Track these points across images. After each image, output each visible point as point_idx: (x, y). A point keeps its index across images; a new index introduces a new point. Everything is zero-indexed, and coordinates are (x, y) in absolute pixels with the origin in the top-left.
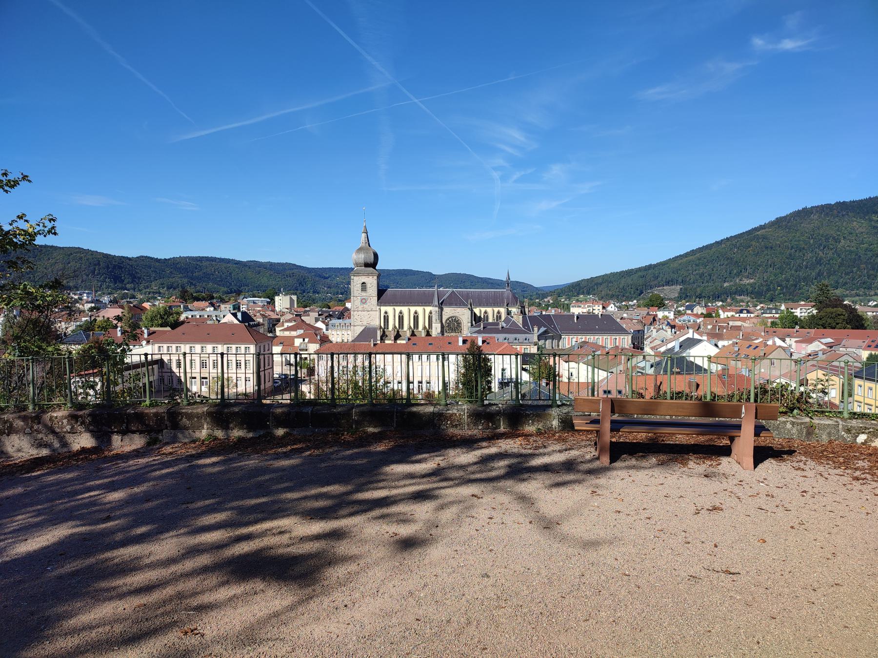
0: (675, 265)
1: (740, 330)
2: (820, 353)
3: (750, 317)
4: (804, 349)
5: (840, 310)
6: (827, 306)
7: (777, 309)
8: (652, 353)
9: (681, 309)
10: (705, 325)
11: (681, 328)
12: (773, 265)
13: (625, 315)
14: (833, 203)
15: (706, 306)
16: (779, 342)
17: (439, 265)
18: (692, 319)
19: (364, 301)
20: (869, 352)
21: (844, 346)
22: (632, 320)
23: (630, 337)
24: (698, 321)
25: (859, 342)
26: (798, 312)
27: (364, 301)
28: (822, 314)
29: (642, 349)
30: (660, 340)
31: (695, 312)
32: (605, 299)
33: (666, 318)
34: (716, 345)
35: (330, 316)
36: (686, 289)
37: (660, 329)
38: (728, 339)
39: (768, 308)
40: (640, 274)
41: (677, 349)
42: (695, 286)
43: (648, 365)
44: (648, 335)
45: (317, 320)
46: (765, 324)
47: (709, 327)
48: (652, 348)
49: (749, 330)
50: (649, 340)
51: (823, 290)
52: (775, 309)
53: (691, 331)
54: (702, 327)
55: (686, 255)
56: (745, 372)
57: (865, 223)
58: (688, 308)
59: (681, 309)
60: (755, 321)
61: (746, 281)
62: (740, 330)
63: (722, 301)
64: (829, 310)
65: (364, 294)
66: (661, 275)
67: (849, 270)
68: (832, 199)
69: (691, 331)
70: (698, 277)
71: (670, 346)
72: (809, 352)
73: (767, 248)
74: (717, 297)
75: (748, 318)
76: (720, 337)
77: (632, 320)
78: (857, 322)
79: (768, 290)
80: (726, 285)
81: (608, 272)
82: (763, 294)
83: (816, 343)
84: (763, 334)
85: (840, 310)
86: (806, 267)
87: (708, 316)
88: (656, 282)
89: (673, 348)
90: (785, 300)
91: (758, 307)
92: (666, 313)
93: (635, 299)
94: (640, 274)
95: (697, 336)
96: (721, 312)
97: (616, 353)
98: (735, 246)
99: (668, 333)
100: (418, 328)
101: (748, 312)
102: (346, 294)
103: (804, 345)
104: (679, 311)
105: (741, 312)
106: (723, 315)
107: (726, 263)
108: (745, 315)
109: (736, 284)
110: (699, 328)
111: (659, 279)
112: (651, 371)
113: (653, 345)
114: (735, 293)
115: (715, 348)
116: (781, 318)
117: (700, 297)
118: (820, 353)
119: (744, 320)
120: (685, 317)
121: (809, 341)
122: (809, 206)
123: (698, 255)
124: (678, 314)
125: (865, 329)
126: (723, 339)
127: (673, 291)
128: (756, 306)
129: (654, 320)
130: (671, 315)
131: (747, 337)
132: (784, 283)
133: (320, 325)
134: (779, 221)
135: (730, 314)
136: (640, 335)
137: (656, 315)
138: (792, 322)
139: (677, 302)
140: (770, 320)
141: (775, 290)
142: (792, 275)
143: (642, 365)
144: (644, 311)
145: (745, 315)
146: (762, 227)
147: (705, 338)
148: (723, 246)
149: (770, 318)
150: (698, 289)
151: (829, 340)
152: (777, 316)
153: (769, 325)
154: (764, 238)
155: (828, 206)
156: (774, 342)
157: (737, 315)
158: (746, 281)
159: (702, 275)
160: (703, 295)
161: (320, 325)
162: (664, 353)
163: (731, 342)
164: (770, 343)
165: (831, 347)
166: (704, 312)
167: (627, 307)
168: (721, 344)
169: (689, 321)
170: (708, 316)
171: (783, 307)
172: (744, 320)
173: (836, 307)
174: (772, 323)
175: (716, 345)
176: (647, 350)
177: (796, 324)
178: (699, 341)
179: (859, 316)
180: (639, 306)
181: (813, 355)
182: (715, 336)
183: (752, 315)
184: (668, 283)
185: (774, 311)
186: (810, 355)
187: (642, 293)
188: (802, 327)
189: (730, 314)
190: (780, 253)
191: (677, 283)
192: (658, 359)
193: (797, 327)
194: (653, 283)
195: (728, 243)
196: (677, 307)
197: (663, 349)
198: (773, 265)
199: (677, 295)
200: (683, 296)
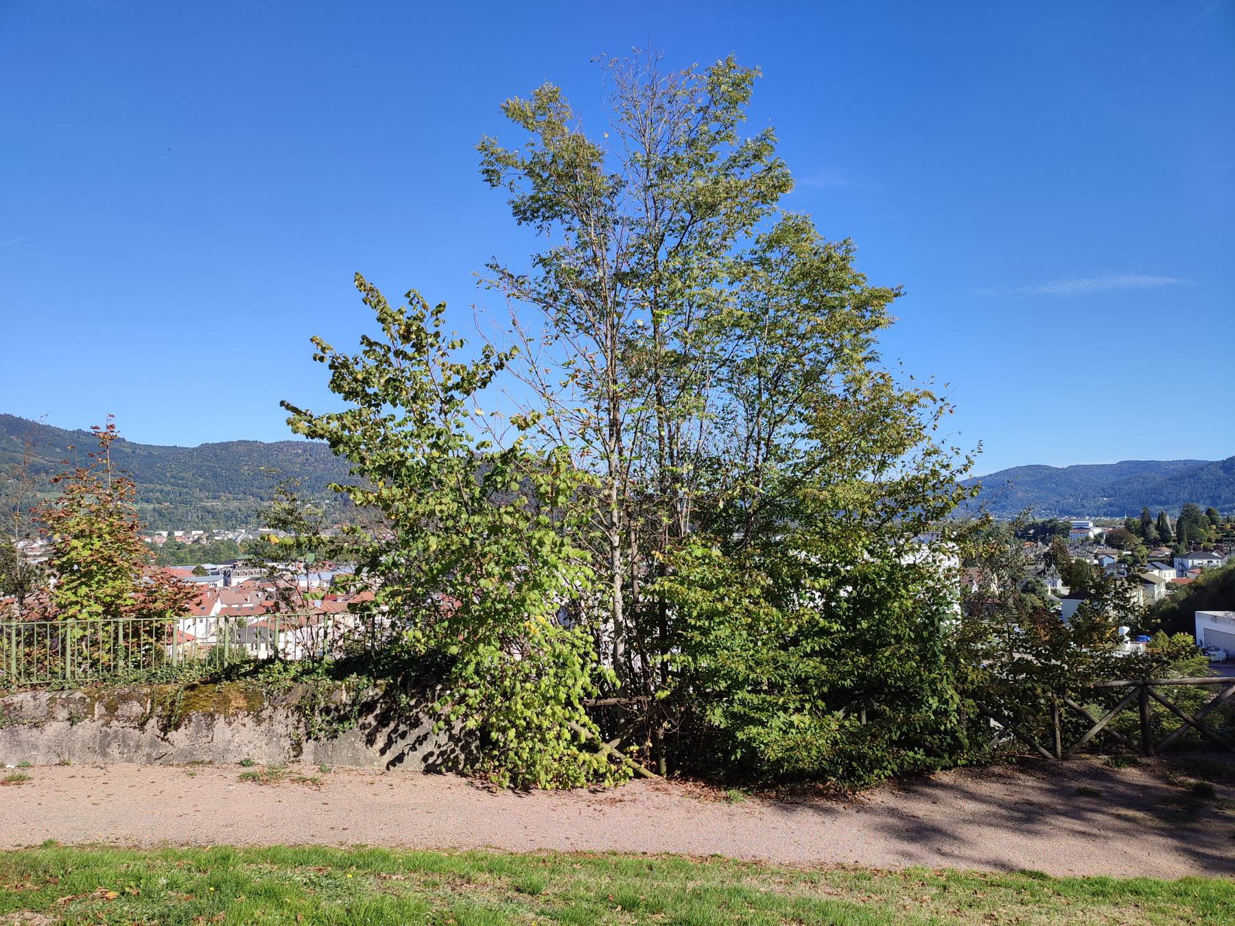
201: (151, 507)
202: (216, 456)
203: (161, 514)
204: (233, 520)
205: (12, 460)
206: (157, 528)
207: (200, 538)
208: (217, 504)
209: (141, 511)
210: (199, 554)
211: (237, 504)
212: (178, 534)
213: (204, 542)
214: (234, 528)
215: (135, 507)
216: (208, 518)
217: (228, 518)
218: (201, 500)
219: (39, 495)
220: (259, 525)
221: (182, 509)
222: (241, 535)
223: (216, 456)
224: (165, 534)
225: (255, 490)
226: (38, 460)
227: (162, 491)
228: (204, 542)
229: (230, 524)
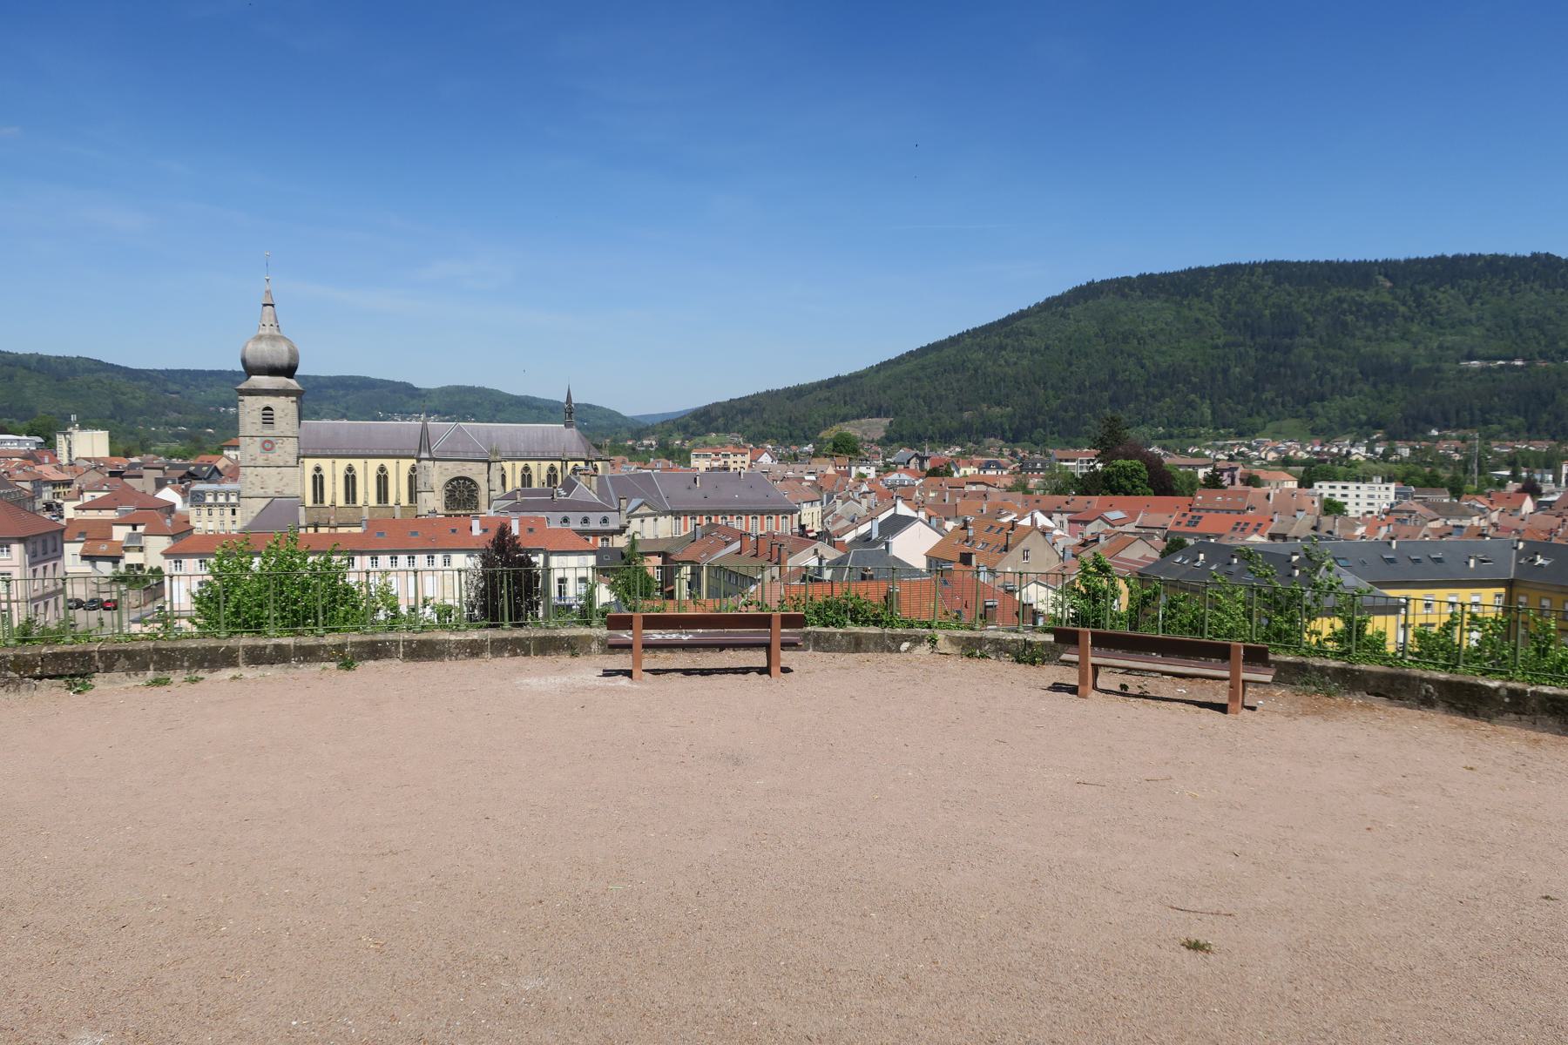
14: (1134, 276)
17: (428, 377)
19: (268, 445)
27: (268, 445)
32: (757, 439)
35: (192, 476)
37: (849, 498)
45: (160, 484)
55: (900, 360)
65: (268, 432)
68: (1132, 270)
74: (947, 439)
81: (762, 390)
92: (863, 470)
100: (386, 501)
102: (229, 432)
105: (987, 466)
122: (1097, 280)
127: (878, 427)
130: (871, 472)
133: (168, 495)
134: (1050, 304)
146: (1022, 315)
155: (1127, 281)
161: (168, 495)
167: (795, 458)
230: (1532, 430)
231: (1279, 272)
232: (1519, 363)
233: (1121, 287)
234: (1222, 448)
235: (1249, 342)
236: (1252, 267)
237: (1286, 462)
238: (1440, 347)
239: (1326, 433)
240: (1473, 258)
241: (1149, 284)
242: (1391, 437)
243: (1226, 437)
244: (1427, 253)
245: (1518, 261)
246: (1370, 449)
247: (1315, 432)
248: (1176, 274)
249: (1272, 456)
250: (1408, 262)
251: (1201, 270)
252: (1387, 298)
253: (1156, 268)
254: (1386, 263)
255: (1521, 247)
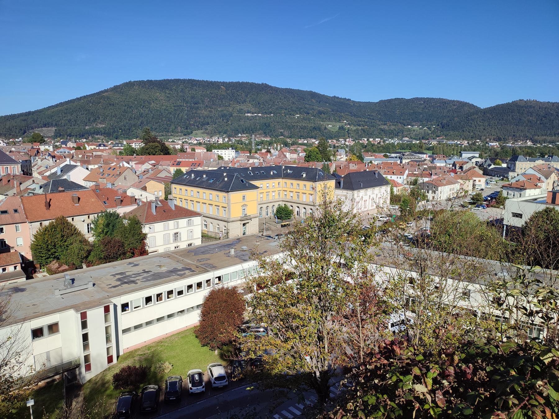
0: (49, 112)
1: (101, 157)
2: (150, 170)
3: (106, 149)
4: (140, 168)
5: (157, 144)
6: (150, 142)
7: (122, 144)
8: (40, 177)
9: (58, 144)
10: (77, 155)
11: (60, 157)
12: (115, 116)
13: (13, 149)
15: (75, 142)
16: (126, 165)
18: (67, 151)
20: (175, 168)
21: (161, 165)
22: (19, 152)
23: (19, 166)
24: (71, 152)
25: (168, 162)
26: (133, 145)
28: (148, 146)
29: (31, 174)
30: (44, 167)
31: (68, 146)
33: (47, 150)
34: (87, 169)
36: (59, 130)
38: (94, 164)
39: (116, 143)
40: (22, 118)
41: (59, 173)
42: (66, 128)
43: (37, 187)
44: (34, 164)
46: (117, 155)
47: (80, 156)
48: (39, 173)
49: (107, 158)
50: (36, 167)
51: (147, 132)
52: (121, 144)
53: (68, 159)
54: (75, 156)
55: (57, 106)
56: (109, 186)
57: (163, 94)
58: (63, 143)
59: (58, 144)
60: (109, 151)
61: (100, 126)
62: (101, 157)
63: (86, 139)
64: (151, 144)
66: (39, 119)
67: (157, 121)
69: (68, 159)
70: (67, 122)
71: (53, 171)
72: (143, 170)
73: (110, 104)
74: (82, 136)
75: (106, 150)
76: (88, 162)
77: (19, 152)
78: (166, 151)
79: (114, 132)
80: (87, 128)
82: (112, 134)
83: (146, 164)
84: (115, 159)
85: (157, 144)
86: (135, 118)
87: (78, 148)
88: (36, 125)
89: (56, 172)
90: (125, 138)
91: (110, 143)
92: (47, 147)
93: (20, 136)
94: (22, 118)
95: (72, 163)
96: (86, 145)
97: (10, 179)
98: (90, 102)
99: (51, 161)
101: (104, 146)
103: (140, 165)
104: (56, 146)
105: (100, 145)
106: (88, 148)
107: (85, 113)
108: (103, 148)
109: (93, 128)
110: (73, 157)
111: (38, 122)
112: (41, 191)
113: (39, 171)
114: (94, 133)
115: (87, 170)
116: (125, 150)
117: (70, 135)
118: (150, 170)
119: (102, 151)
120: (62, 150)
121: (143, 163)
123: (65, 106)
124: (56, 147)
125: (170, 154)
126: (90, 164)
128: (108, 142)
129: (38, 152)
130: (51, 149)
131: (106, 162)
132: (123, 128)
135: (93, 147)
136: (28, 164)
137: (39, 149)
138: (132, 152)
139: (54, 139)
140: (118, 151)
141: (118, 132)
142: (127, 123)
143: (32, 187)
144: (29, 146)
145: (103, 148)
146: (106, 91)
147: (79, 164)
148: (82, 101)
149: (118, 149)
150: (68, 130)
151: (153, 162)
152: (122, 148)
153: (118, 154)
154: (108, 98)
156: (123, 165)
157: (98, 148)
158: (100, 126)
159: (70, 121)
160: (72, 134)
162: (49, 176)
163: (96, 166)
164: (121, 164)
165: (154, 166)
166: (75, 145)
167: (15, 143)
168: (90, 167)
169: (65, 152)
170: (78, 148)
171: (125, 143)
172: (102, 151)
173: (154, 142)
174: (120, 152)
175: (87, 169)
176: (35, 174)
177: (134, 152)
178: (75, 166)
179: (167, 147)
180: (24, 142)
181: (146, 172)
182: (85, 162)
183: (107, 148)
184: (45, 126)
185: (120, 145)
186: (145, 172)
187: (25, 132)
188: (137, 155)
189: (93, 147)
190: (119, 108)
191: (52, 126)
192: (45, 182)
193: (135, 155)
194: (33, 125)
195: (86, 100)
196: (54, 143)
197: (47, 174)
198: (115, 116)
199: (53, 134)
200: (58, 135)
201: (360, 128)
202: (386, 105)
203: (364, 131)
204: (393, 134)
205: (313, 109)
206: (363, 137)
207: (380, 142)
208: (386, 127)
209: (357, 130)
210: (381, 148)
211: (394, 127)
212: (371, 140)
213: (382, 144)
214: (392, 138)
215: (355, 128)
216: (383, 133)
217: (390, 133)
218: (379, 125)
219: (322, 123)
220: (403, 137)
221: (372, 129)
222: (396, 141)
223: (386, 105)
224: (366, 139)
225: (401, 121)
226: (321, 109)
227: (364, 121)
228: (382, 144)
229: (391, 136)
230: (266, 136)
231: (192, 83)
232: (260, 115)
233: (141, 84)
234: (180, 139)
235: (185, 105)
236: (184, 81)
237: (200, 144)
238: (240, 109)
239: (211, 135)
240: (247, 83)
241: (151, 84)
242: (229, 137)
243: (181, 136)
244: (235, 80)
245: (259, 85)
246: (224, 140)
247: (208, 134)
248: (160, 81)
249: (195, 142)
250: (229, 82)
251: (168, 80)
252: (224, 93)
253: (153, 78)
254: (224, 83)
255: (258, 81)
